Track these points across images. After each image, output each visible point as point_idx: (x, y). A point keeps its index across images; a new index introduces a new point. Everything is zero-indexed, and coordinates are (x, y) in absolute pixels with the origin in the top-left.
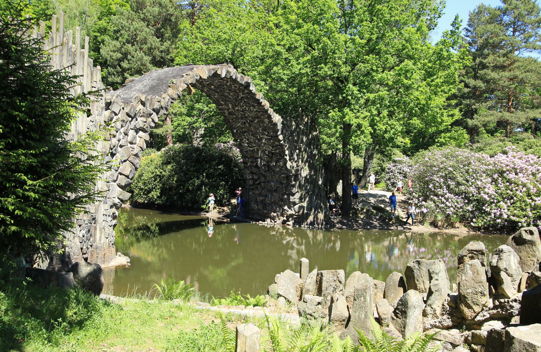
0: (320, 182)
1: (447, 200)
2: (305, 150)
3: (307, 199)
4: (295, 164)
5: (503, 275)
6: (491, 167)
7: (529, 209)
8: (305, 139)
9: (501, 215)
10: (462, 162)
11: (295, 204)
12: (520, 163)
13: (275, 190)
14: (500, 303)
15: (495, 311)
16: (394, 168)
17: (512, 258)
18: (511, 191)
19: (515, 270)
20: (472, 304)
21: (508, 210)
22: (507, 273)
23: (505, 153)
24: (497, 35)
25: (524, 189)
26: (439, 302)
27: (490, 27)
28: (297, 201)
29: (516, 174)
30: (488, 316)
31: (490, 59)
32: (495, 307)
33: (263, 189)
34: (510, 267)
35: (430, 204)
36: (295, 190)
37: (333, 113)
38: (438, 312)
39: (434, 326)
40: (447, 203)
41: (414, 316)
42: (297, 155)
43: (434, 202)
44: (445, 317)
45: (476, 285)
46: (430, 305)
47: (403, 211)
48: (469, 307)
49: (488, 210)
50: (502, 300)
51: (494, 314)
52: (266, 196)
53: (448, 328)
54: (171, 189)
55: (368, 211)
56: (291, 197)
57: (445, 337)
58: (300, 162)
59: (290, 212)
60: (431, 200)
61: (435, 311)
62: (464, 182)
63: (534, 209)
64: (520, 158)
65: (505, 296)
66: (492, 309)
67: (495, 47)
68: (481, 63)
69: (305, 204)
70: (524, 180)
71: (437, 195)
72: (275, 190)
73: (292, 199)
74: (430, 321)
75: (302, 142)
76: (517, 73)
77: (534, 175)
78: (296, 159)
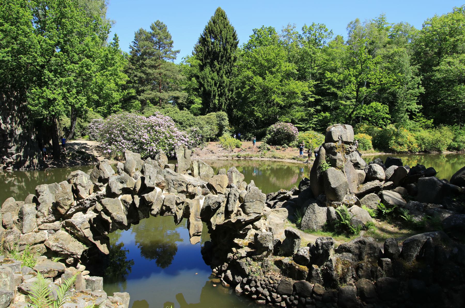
0: (33, 138)
1: (123, 143)
2: (17, 116)
3: (23, 150)
4: (9, 126)
5: (79, 187)
6: (146, 124)
7: (166, 145)
8: (16, 108)
9: (153, 150)
10: (130, 122)
11: (12, 154)
12: (161, 121)
14: (80, 202)
15: (78, 207)
16: (93, 126)
17: (84, 177)
18: (157, 136)
19: (86, 183)
20: (63, 206)
21: (156, 147)
23: (154, 115)
24: (150, 48)
25: (164, 135)
26: (46, 208)
27: (146, 43)
28: (14, 152)
29: (160, 127)
30: (74, 210)
31: (148, 62)
32: (78, 205)
34: (83, 182)
35: (113, 147)
36: (11, 144)
37: (35, 90)
40: (123, 146)
41: (30, 220)
42: (11, 119)
43: (116, 145)
44: (50, 216)
45: (64, 195)
46: (39, 211)
48: (62, 208)
49: (146, 148)
50: (81, 201)
53: (53, 221)
55: (73, 154)
56: (8, 150)
57: (50, 227)
58: (14, 124)
59: (9, 160)
60: (114, 144)
61: (44, 213)
62: (132, 133)
63: (169, 145)
64: (162, 118)
65: (82, 198)
67: (151, 54)
68: (143, 64)
69: (21, 154)
70: (164, 130)
71: (117, 141)
73: (9, 151)
74: (41, 220)
75: (14, 110)
76: (162, 71)
77: (169, 127)
78: (10, 122)
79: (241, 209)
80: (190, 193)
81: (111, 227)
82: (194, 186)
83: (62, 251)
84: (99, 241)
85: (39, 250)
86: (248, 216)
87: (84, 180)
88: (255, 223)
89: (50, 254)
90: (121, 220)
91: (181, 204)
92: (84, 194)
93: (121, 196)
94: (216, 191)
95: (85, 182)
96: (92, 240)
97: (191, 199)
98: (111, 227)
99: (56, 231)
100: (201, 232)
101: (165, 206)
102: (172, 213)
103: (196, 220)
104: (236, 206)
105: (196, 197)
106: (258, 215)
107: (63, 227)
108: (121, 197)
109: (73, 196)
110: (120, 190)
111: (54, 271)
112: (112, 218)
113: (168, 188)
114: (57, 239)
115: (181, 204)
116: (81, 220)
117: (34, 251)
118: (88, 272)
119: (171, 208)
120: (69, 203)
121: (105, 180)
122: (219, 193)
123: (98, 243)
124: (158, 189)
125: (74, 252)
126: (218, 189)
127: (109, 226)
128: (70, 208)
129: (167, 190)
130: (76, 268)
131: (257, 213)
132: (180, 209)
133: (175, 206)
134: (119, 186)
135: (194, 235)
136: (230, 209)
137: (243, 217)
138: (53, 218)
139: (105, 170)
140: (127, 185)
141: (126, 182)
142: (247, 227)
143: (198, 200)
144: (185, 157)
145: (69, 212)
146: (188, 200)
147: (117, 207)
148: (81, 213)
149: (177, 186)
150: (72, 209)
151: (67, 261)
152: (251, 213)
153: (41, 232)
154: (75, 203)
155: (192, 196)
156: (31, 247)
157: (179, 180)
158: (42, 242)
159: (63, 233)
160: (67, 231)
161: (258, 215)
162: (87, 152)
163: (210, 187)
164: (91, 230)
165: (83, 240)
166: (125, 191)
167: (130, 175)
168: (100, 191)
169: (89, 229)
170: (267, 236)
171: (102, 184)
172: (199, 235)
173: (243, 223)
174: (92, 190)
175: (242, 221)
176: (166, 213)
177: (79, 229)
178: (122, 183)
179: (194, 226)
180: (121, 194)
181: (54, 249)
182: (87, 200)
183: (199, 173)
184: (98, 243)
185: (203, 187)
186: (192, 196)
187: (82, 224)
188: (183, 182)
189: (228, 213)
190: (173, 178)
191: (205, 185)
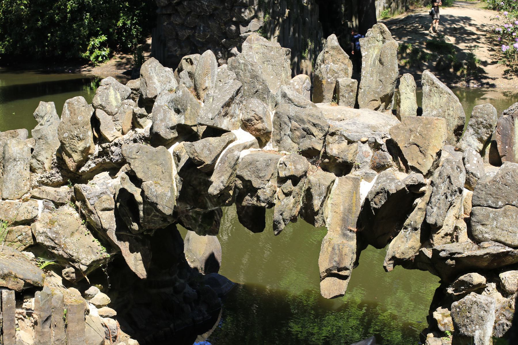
3: (277, 33)
5: (100, 114)
13: (212, 16)
14: (103, 148)
15: (100, 160)
17: (112, 92)
19: (116, 107)
20: (70, 152)
22: (105, 111)
30: (93, 165)
33: (188, 14)
38: (47, 165)
39: (42, 183)
44: (53, 171)
46: (34, 157)
47: (492, 50)
48: (70, 156)
50: (104, 145)
51: (101, 163)
52: (195, 28)
53: (58, 185)
54: (19, 20)
55: (415, 51)
56: (242, 29)
57: (48, 194)
61: (43, 164)
66: (98, 157)
72: (212, 16)
74: (37, 177)
79: (463, 225)
80: (333, 159)
81: (141, 213)
82: (350, 142)
83: (54, 248)
84: (127, 244)
85: (20, 238)
86: (480, 248)
87: (112, 99)
88: (502, 275)
89: (37, 248)
90: (154, 200)
91: (289, 182)
92: (110, 131)
93: (177, 143)
94: (405, 162)
95: (114, 103)
96: (114, 238)
97: (338, 175)
98: (141, 213)
99: (58, 205)
100: (346, 269)
101: (240, 177)
102: (258, 198)
103: (344, 235)
104: (453, 212)
105: (354, 173)
106: (508, 249)
107: (73, 200)
108: (176, 146)
109: (90, 133)
110: (172, 128)
111: (16, 277)
112: (143, 193)
113: (278, 138)
114: (52, 222)
115: (289, 182)
116: (103, 187)
117: (11, 237)
118: (115, 313)
119: (255, 185)
120: (81, 146)
121: (147, 103)
122: (414, 169)
123: (124, 247)
124: (245, 137)
125: (75, 254)
126: (412, 157)
127: (138, 211)
128: (86, 160)
129: (278, 142)
130: (84, 296)
131: (505, 244)
132: (287, 195)
133: (273, 183)
134: (170, 119)
135: (330, 274)
136: (431, 220)
137: (465, 247)
138: (58, 177)
139: (150, 78)
140: (186, 119)
141: (185, 110)
142: (462, 278)
143: (356, 181)
144: (380, 61)
145: (83, 169)
146: (318, 176)
147: (159, 168)
148: (106, 174)
149: (297, 133)
150: (89, 162)
151: (64, 271)
152: (486, 240)
153: (31, 202)
154: (96, 149)
155: (343, 168)
156: (8, 229)
157: (305, 118)
158: (28, 222)
159: (69, 214)
160: (77, 209)
161: (508, 249)
162: (462, 46)
163: (393, 147)
164: (117, 215)
165: (97, 232)
166: (186, 133)
167: (198, 97)
168: (141, 127)
169: (112, 213)
170: (475, 306)
171: (143, 111)
172: (344, 278)
173: (449, 262)
174: (129, 125)
175: (443, 254)
176: (247, 197)
177: (91, 208)
178: (178, 111)
179: (330, 249)
180: (175, 140)
181: (40, 239)
182: (116, 145)
183: (420, 112)
184: (124, 247)
185: (376, 146)
186: (343, 168)
187: (99, 197)
188: (314, 125)
189: (428, 231)
190: (292, 110)
191: (380, 141)
